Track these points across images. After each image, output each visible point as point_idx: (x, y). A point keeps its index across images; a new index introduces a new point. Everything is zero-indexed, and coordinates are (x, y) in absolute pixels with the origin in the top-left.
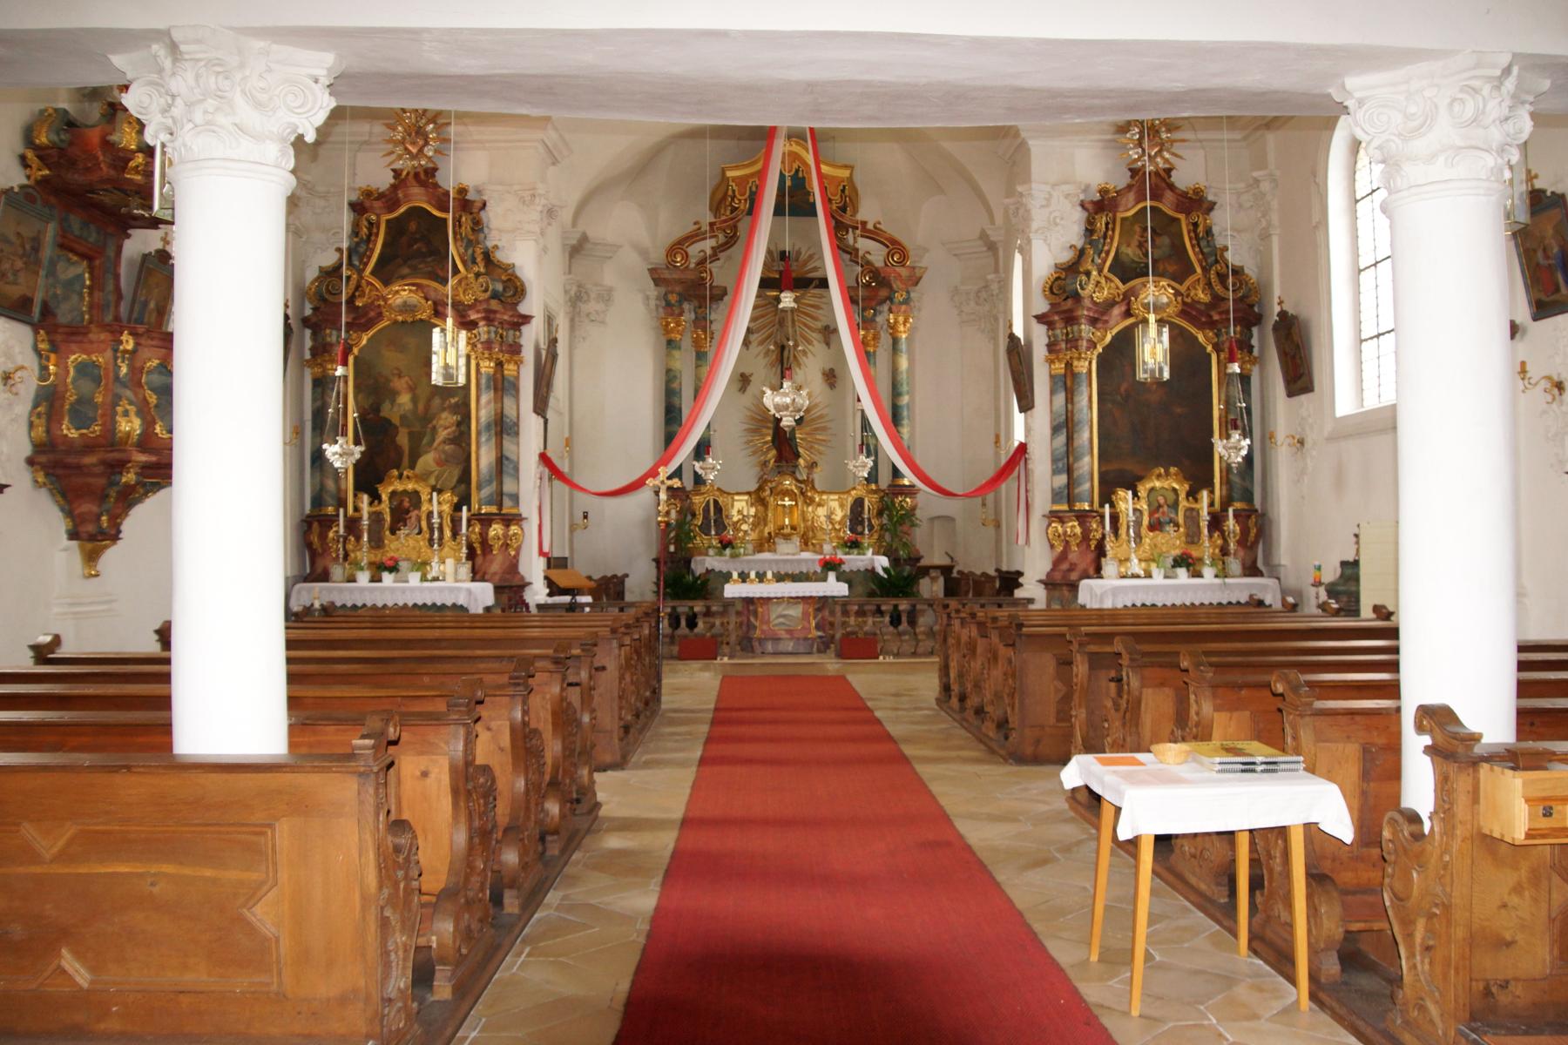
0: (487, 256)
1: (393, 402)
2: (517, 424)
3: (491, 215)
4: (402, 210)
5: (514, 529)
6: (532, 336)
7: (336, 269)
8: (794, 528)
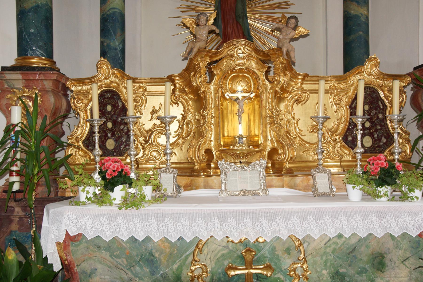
8: (253, 143)
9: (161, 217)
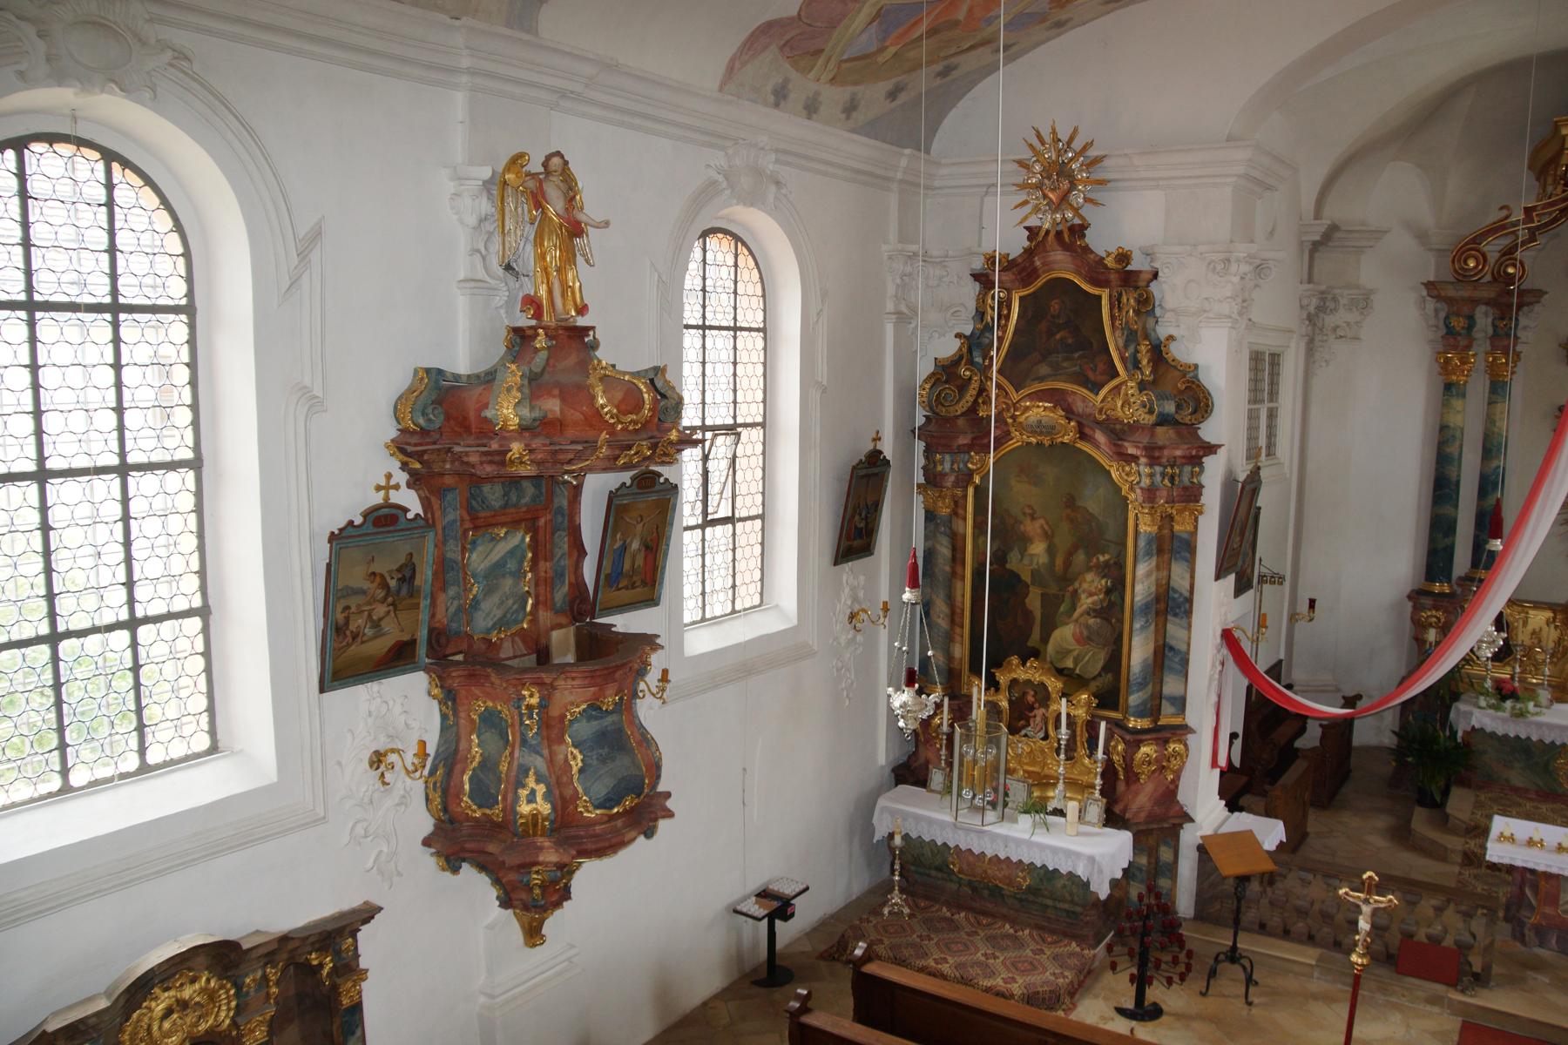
0: (1158, 354)
1: (1023, 551)
2: (1190, 601)
3: (1165, 287)
4: (1040, 283)
5: (1172, 746)
6: (1213, 475)
7: (955, 362)
9: (1540, 725)
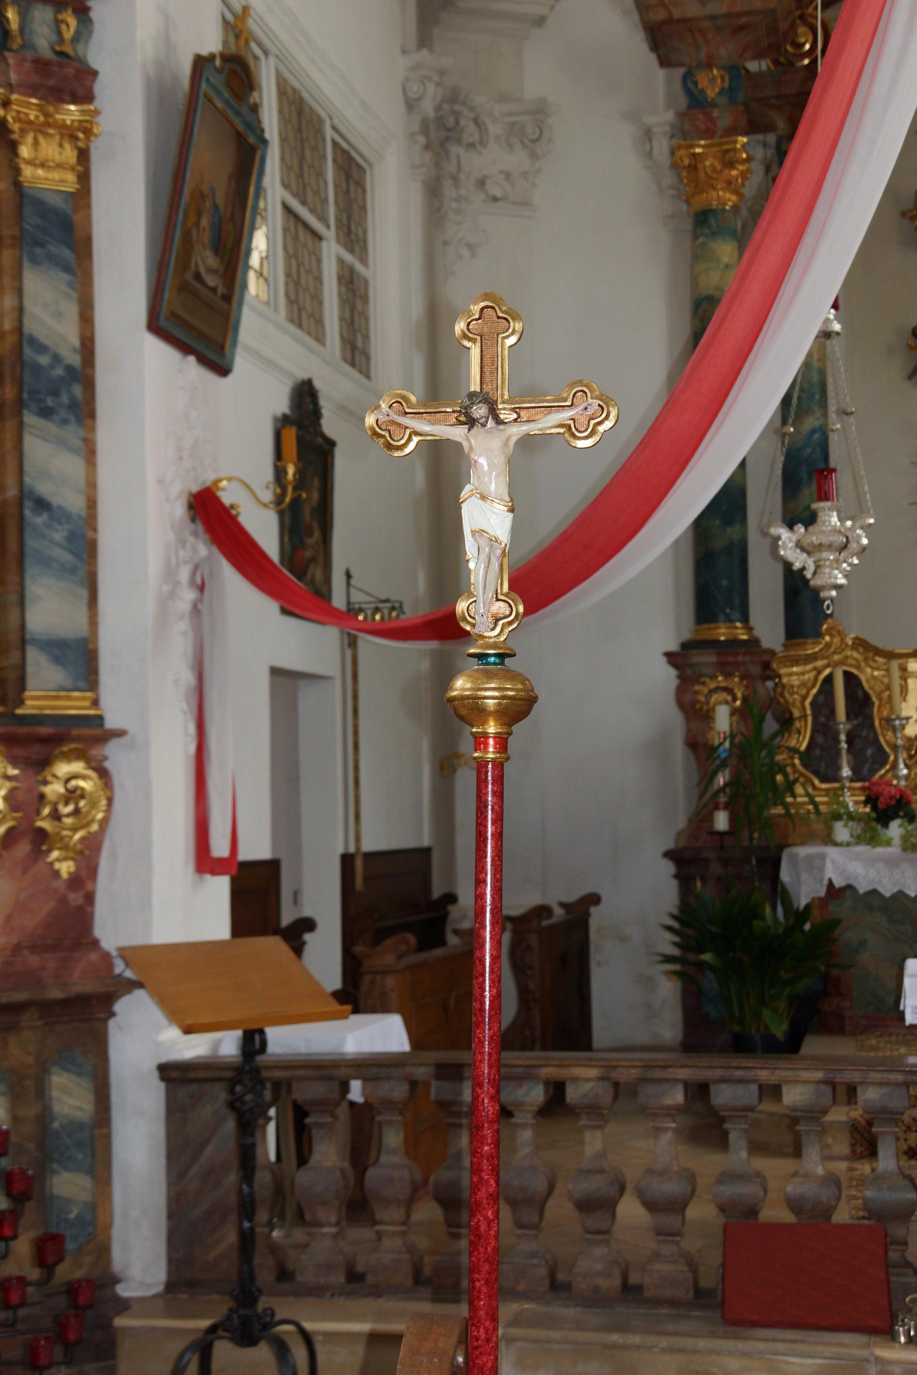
2: (89, 385)
